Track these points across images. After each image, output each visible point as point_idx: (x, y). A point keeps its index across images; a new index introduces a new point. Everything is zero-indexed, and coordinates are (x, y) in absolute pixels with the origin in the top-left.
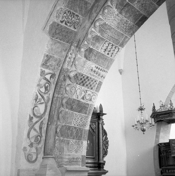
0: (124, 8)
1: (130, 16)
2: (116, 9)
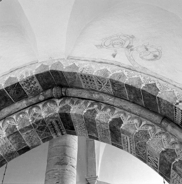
1: (16, 143)
2: (5, 133)
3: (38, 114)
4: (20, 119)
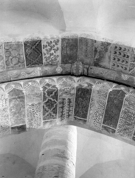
0: (17, 98)
2: (8, 95)
3: (51, 85)
4: (29, 86)
